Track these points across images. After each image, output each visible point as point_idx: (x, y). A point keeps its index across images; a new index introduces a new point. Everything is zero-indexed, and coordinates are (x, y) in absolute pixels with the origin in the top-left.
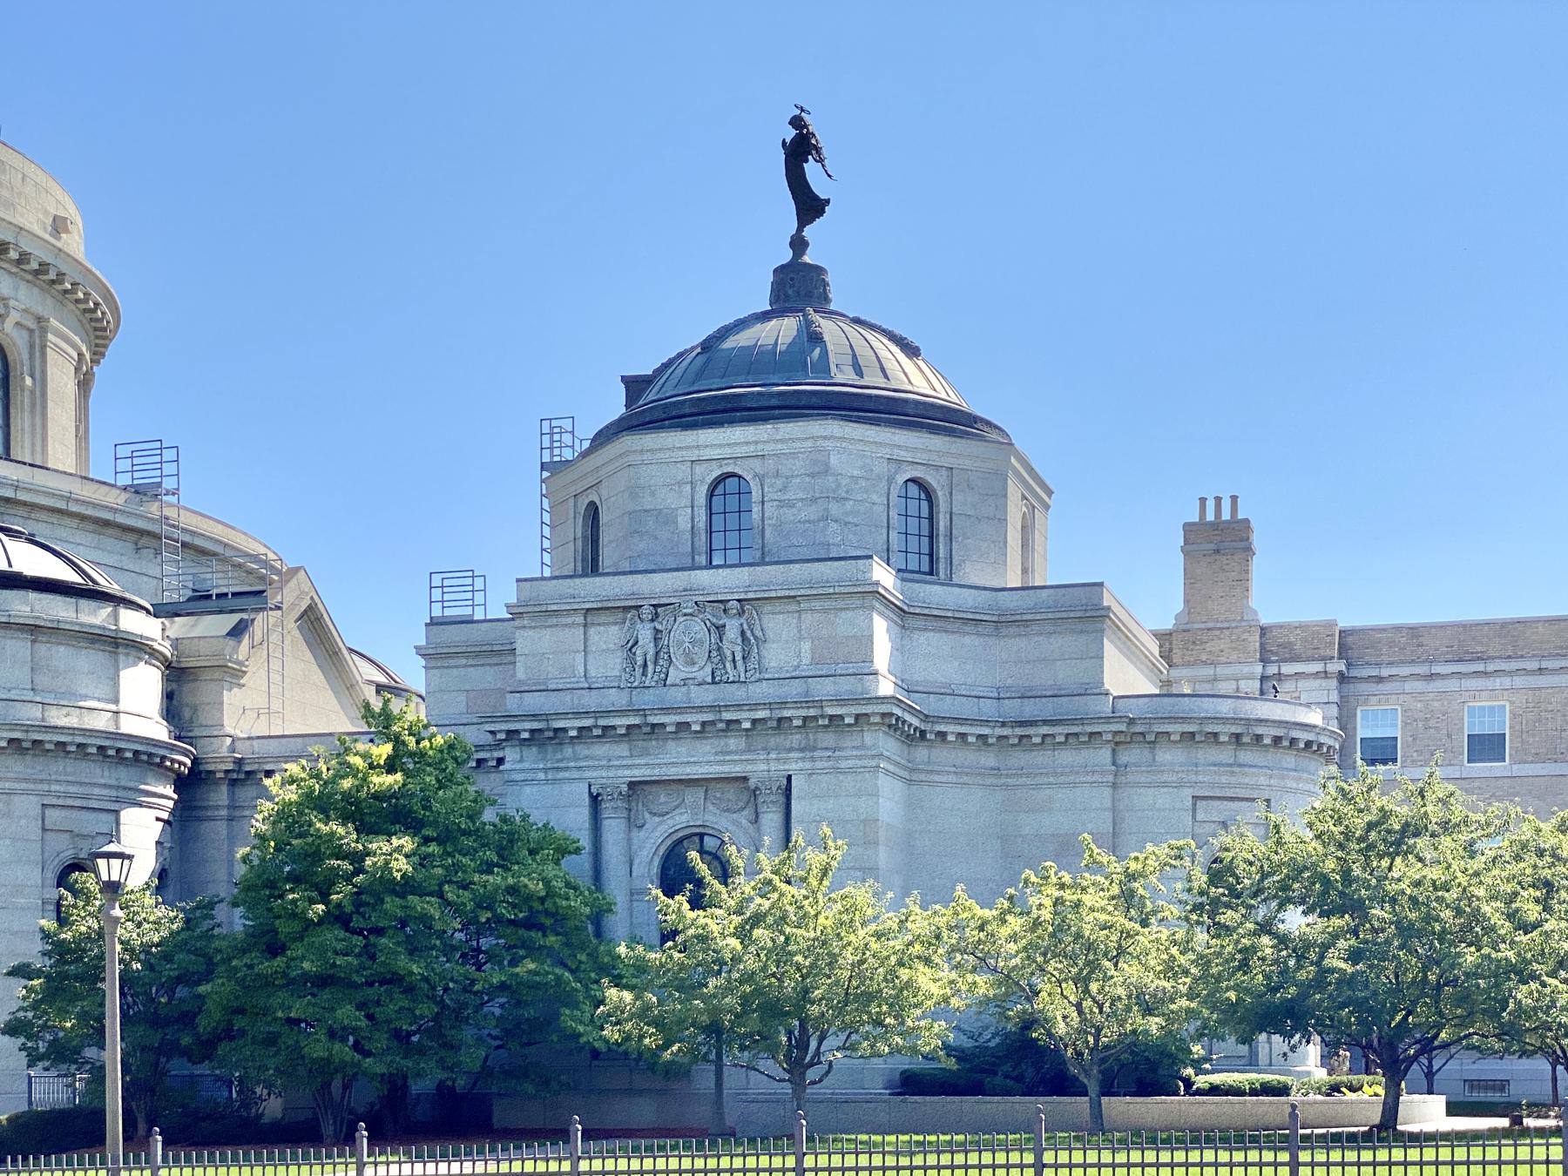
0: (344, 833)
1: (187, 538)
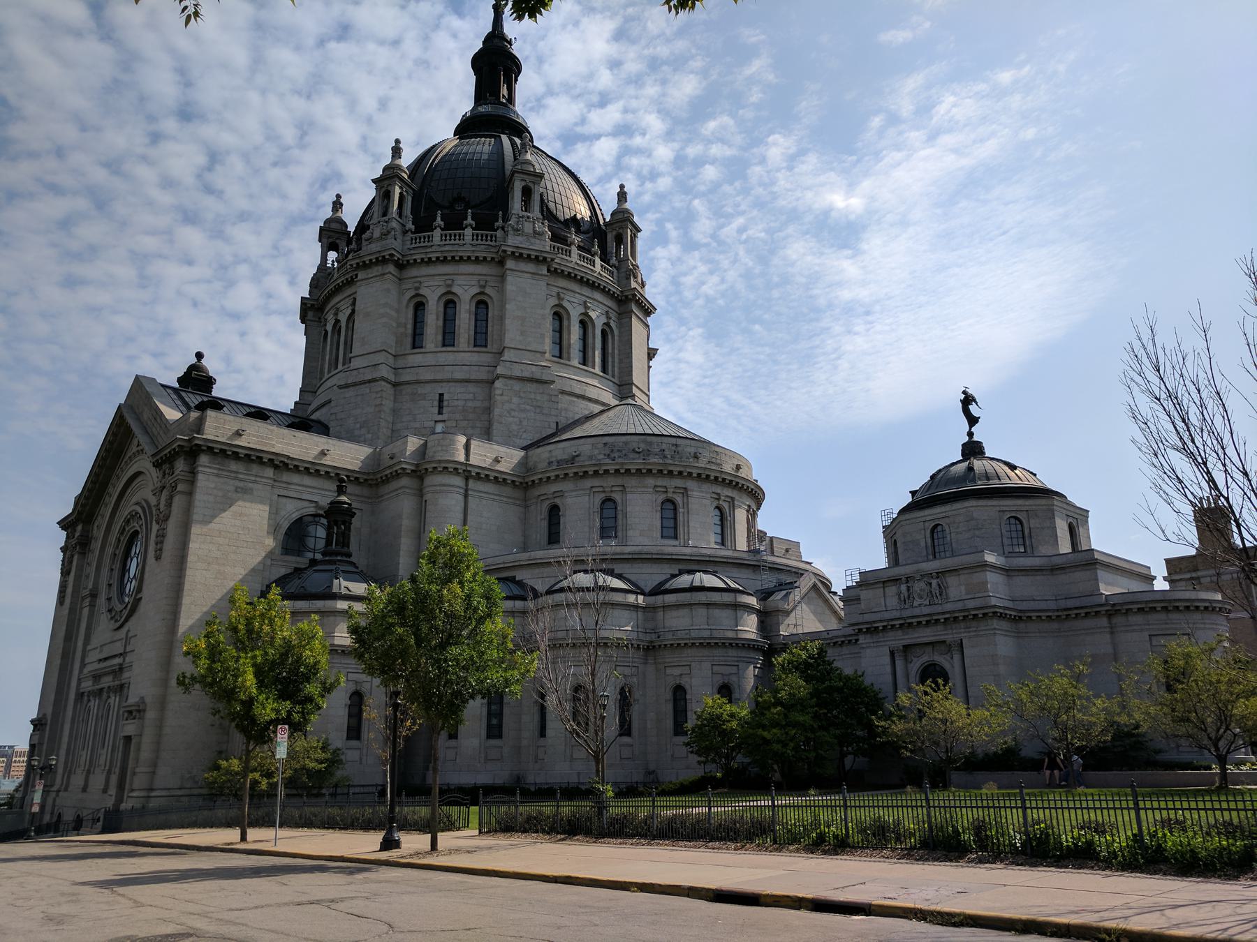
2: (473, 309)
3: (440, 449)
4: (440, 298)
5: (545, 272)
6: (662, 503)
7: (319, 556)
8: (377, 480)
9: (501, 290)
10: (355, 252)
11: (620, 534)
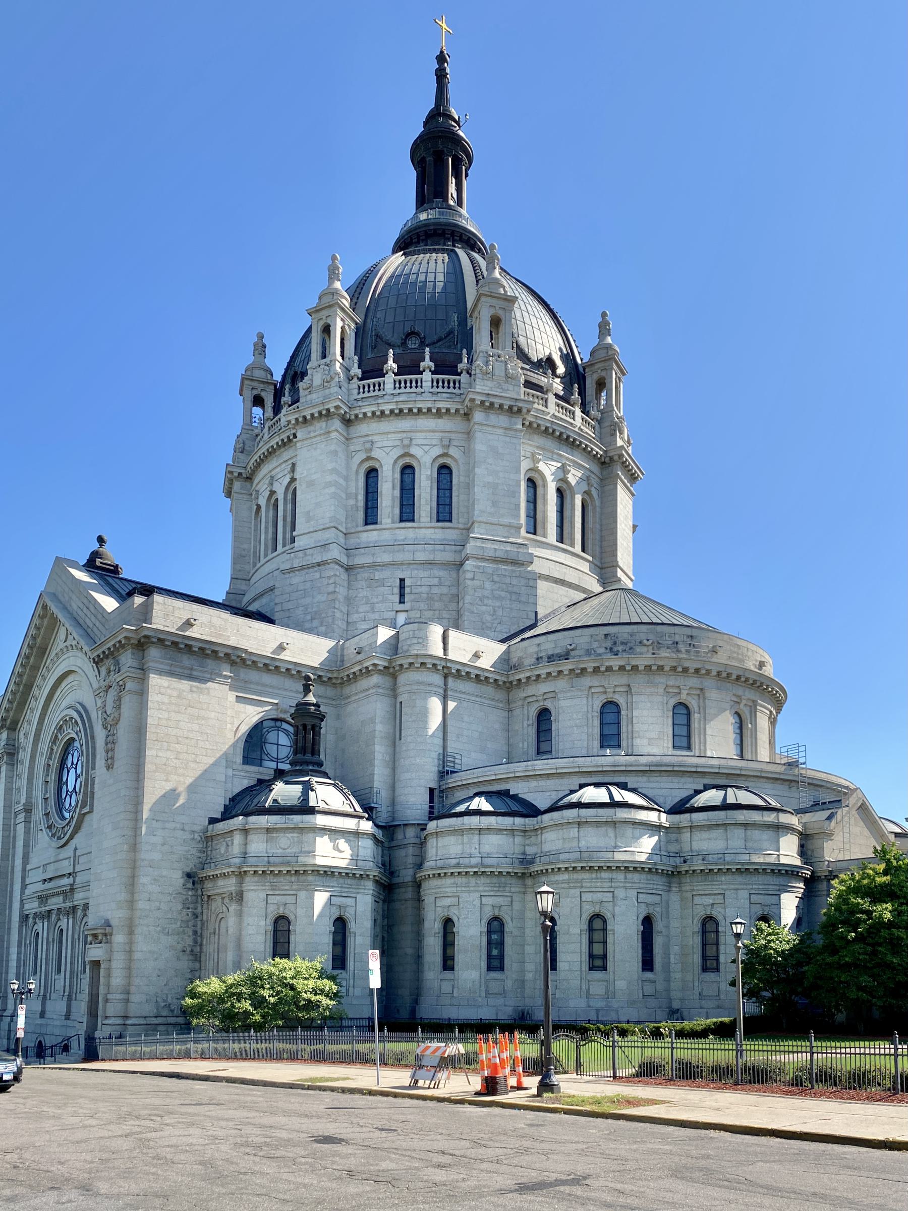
0: (864, 903)
1: (810, 781)
2: (435, 475)
3: (415, 641)
5: (520, 426)
6: (674, 707)
7: (286, 767)
8: (342, 678)
9: (468, 451)
10: (290, 406)
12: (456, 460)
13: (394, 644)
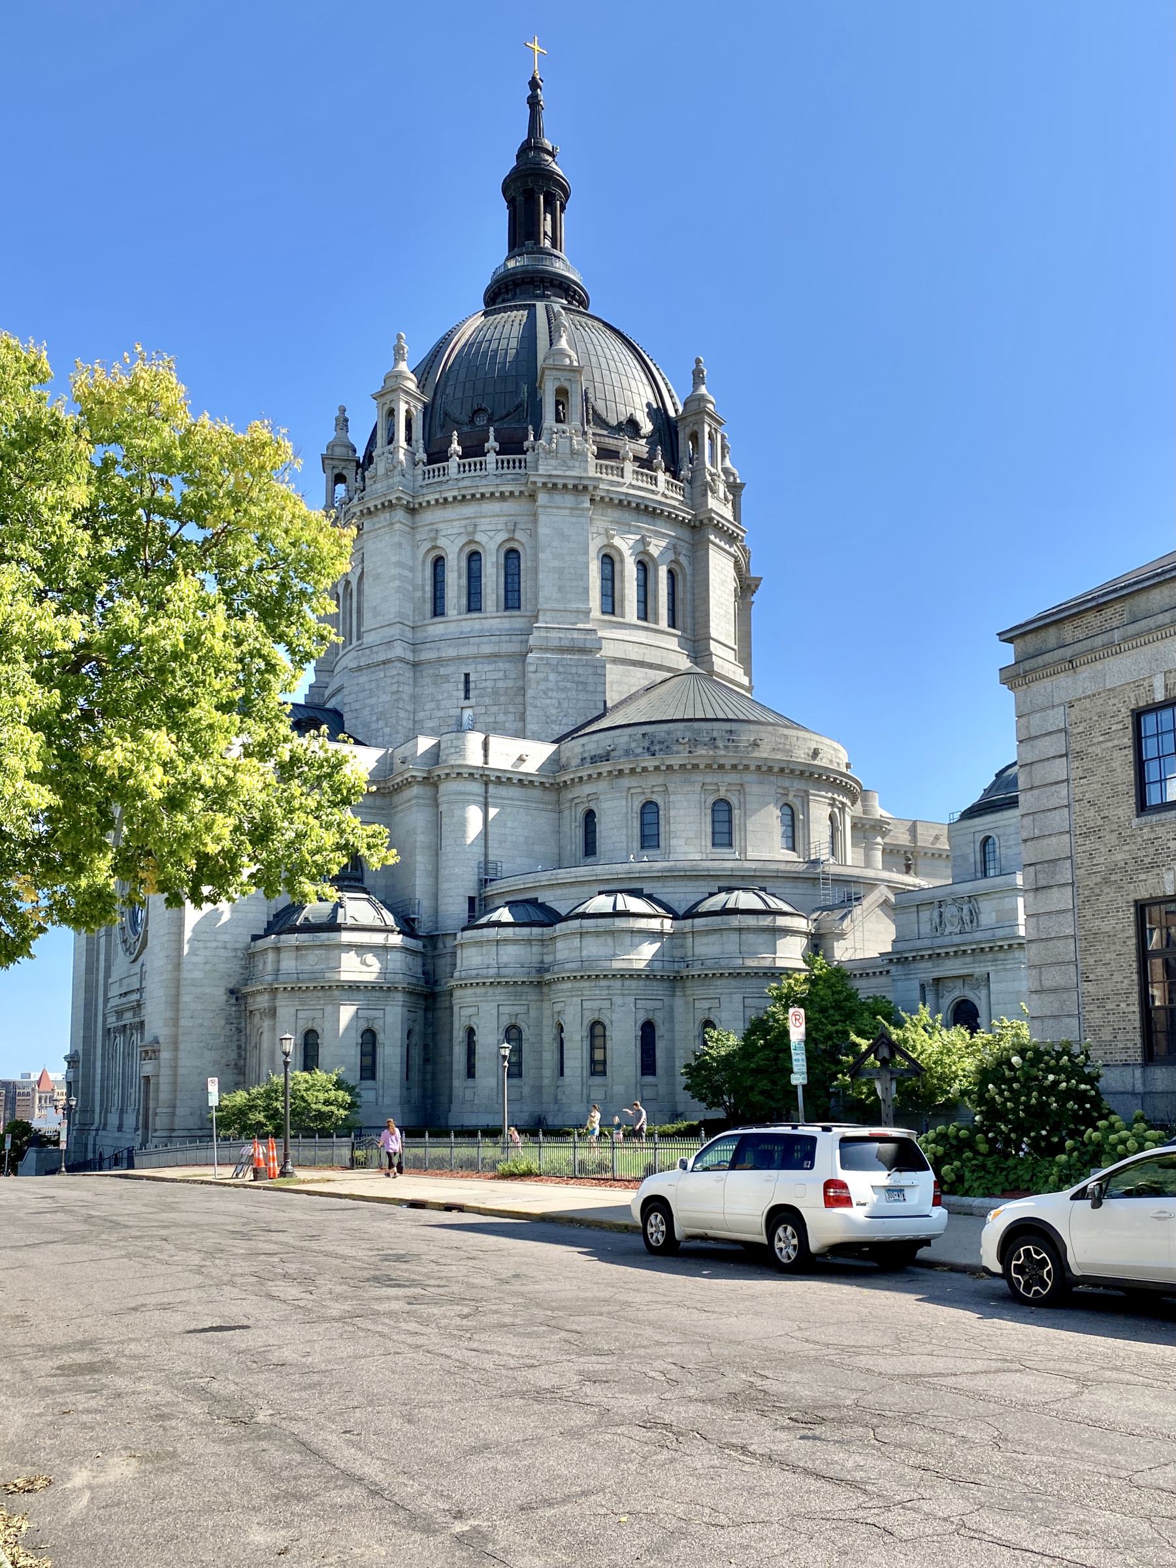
2: (502, 561)
4: (461, 549)
5: (587, 504)
11: (662, 843)
12: (522, 544)
13: (435, 754)
